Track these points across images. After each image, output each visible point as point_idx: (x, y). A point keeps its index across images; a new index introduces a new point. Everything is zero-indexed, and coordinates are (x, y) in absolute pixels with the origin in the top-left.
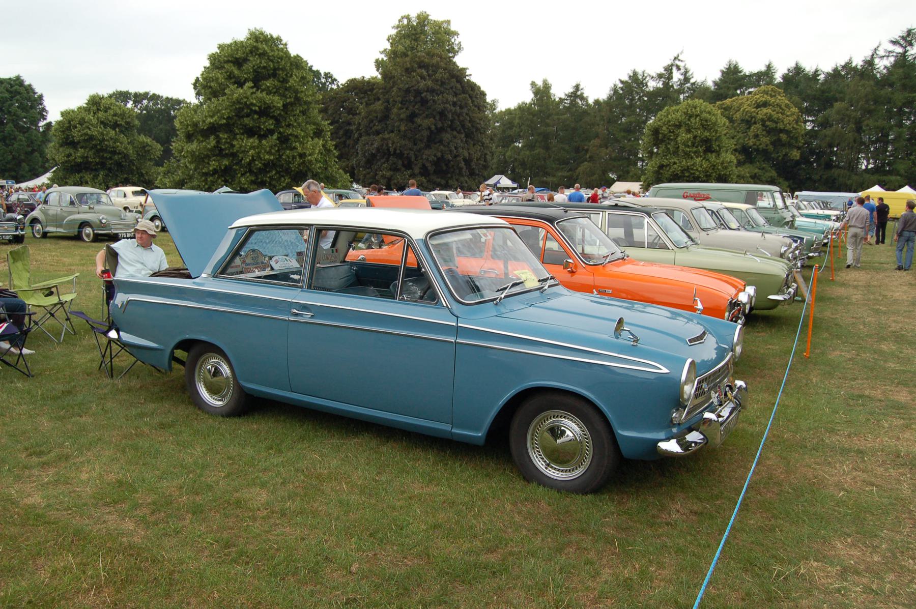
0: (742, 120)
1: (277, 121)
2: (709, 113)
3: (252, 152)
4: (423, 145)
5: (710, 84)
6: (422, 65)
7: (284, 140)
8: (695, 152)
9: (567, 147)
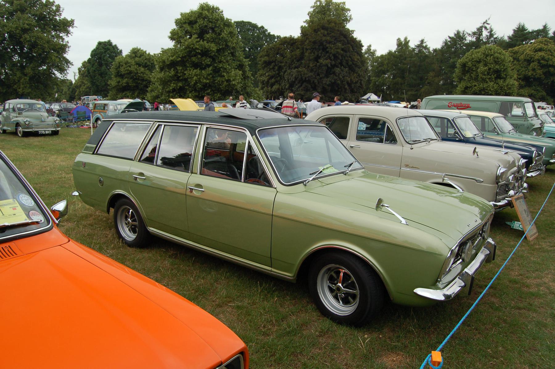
0: (525, 60)
1: (214, 60)
2: (500, 53)
3: (195, 78)
4: (323, 75)
5: (506, 38)
6: (324, 28)
7: (217, 71)
8: (489, 79)
9: (415, 77)
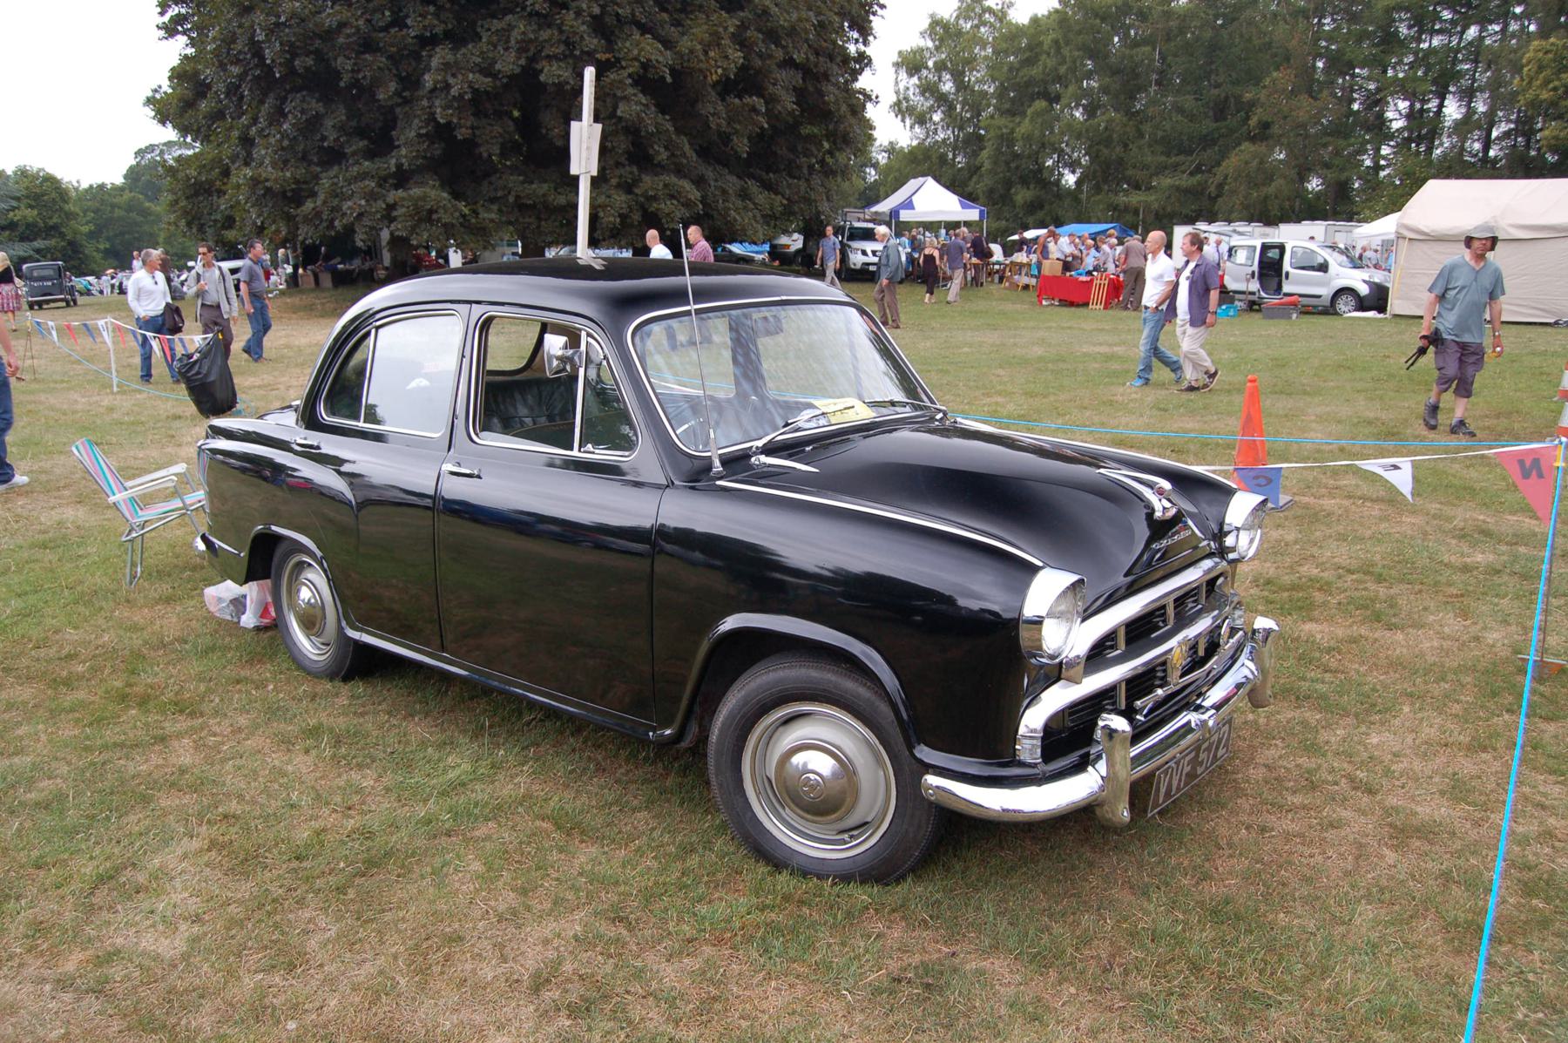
9: (1188, 102)
